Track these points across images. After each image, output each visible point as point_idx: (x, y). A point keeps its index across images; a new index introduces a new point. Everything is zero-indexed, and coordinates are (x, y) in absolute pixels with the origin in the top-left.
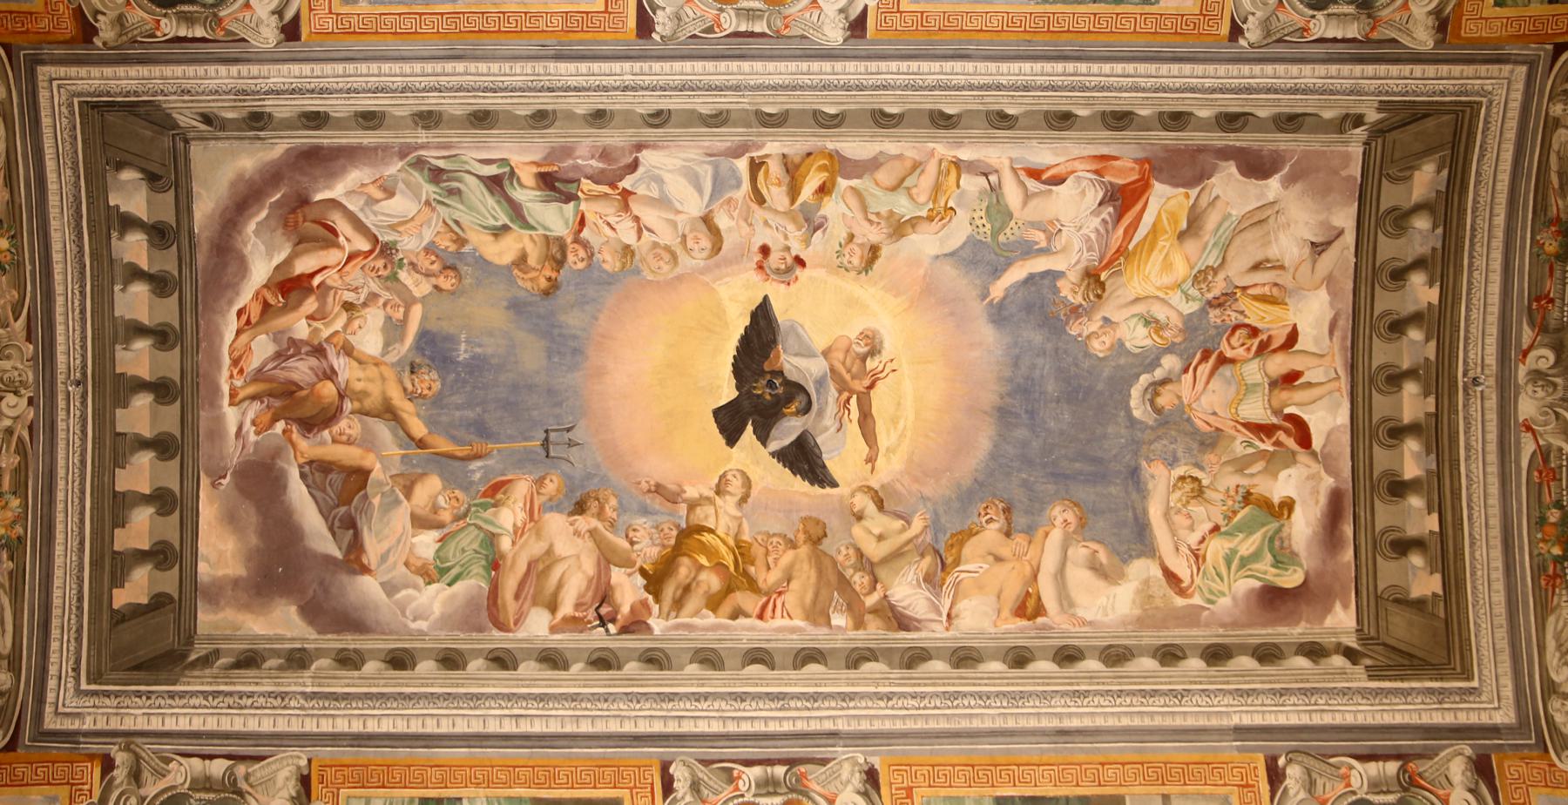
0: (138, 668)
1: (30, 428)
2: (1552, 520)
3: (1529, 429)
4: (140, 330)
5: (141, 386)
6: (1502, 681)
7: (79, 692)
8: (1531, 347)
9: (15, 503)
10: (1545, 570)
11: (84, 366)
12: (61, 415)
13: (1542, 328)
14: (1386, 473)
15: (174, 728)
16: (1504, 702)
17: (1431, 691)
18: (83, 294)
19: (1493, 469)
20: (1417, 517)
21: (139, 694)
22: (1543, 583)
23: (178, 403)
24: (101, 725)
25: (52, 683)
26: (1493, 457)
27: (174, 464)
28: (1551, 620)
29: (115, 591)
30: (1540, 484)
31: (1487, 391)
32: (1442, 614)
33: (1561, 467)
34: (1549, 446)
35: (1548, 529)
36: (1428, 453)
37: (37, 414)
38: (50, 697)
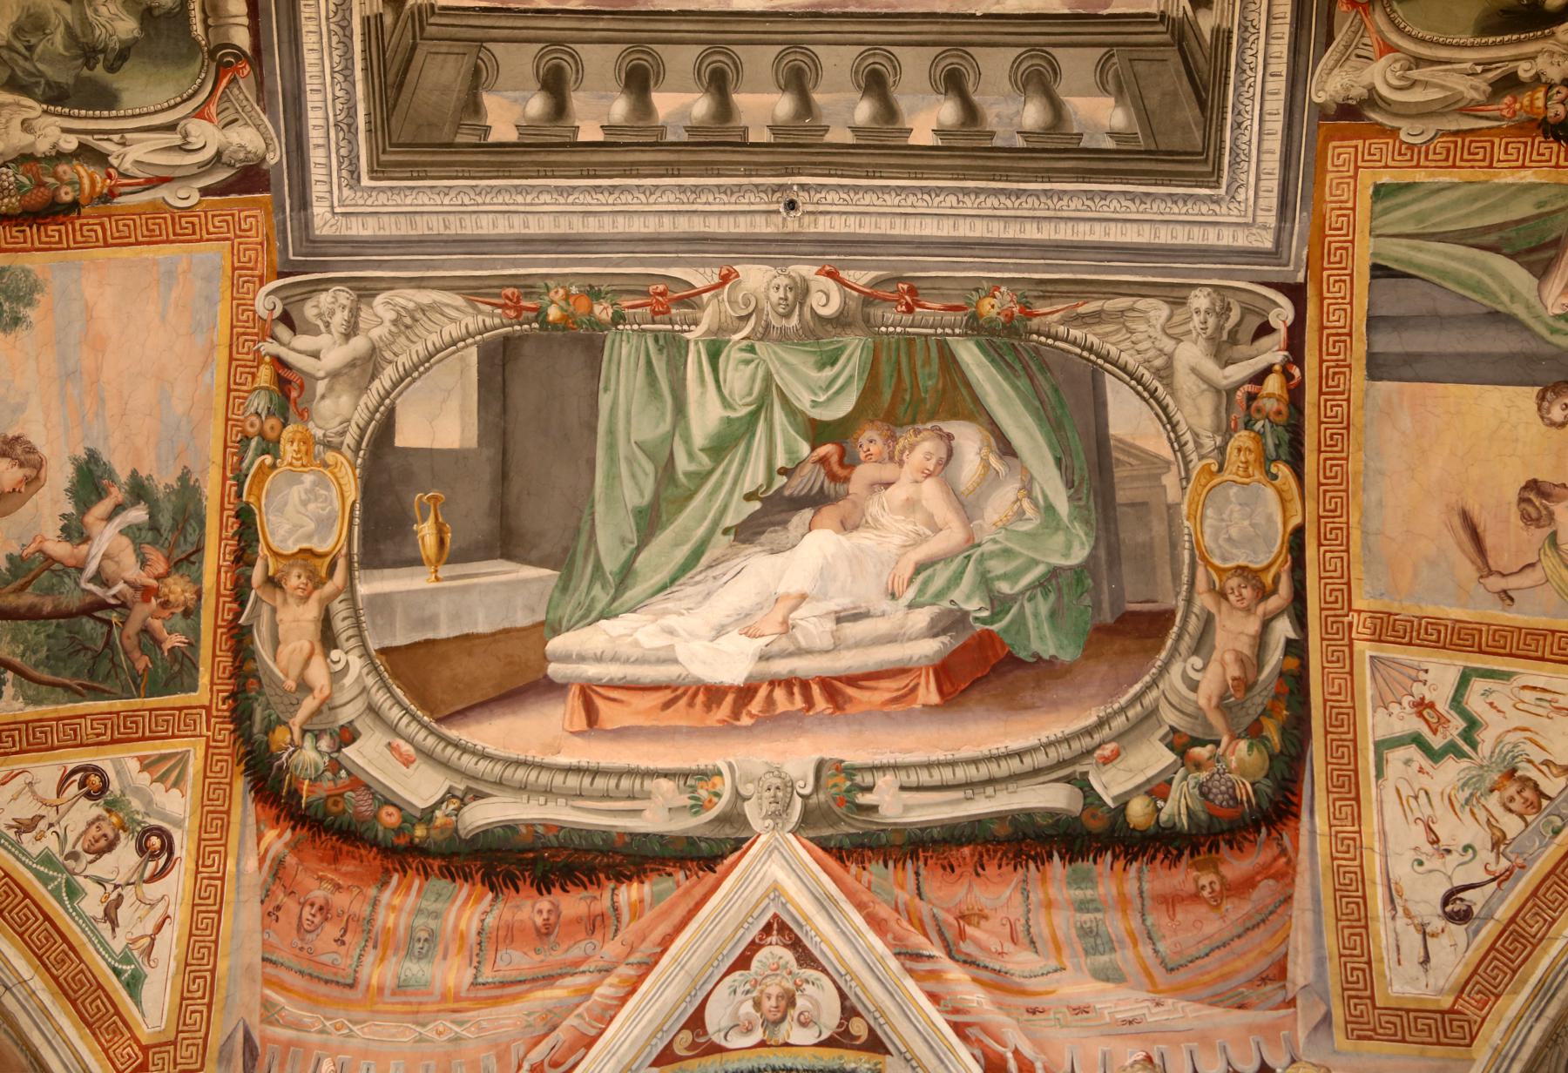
2: (597, 309)
3: (725, 279)
6: (371, 222)
8: (842, 283)
10: (528, 295)
13: (868, 299)
14: (660, 63)
16: (343, 220)
17: (351, 112)
19: (667, 226)
20: (598, 110)
22: (509, 291)
26: (684, 225)
28: (459, 301)
30: (646, 294)
31: (778, 219)
32: (460, 139)
33: (671, 322)
34: (702, 308)
35: (584, 302)
36: (689, 129)
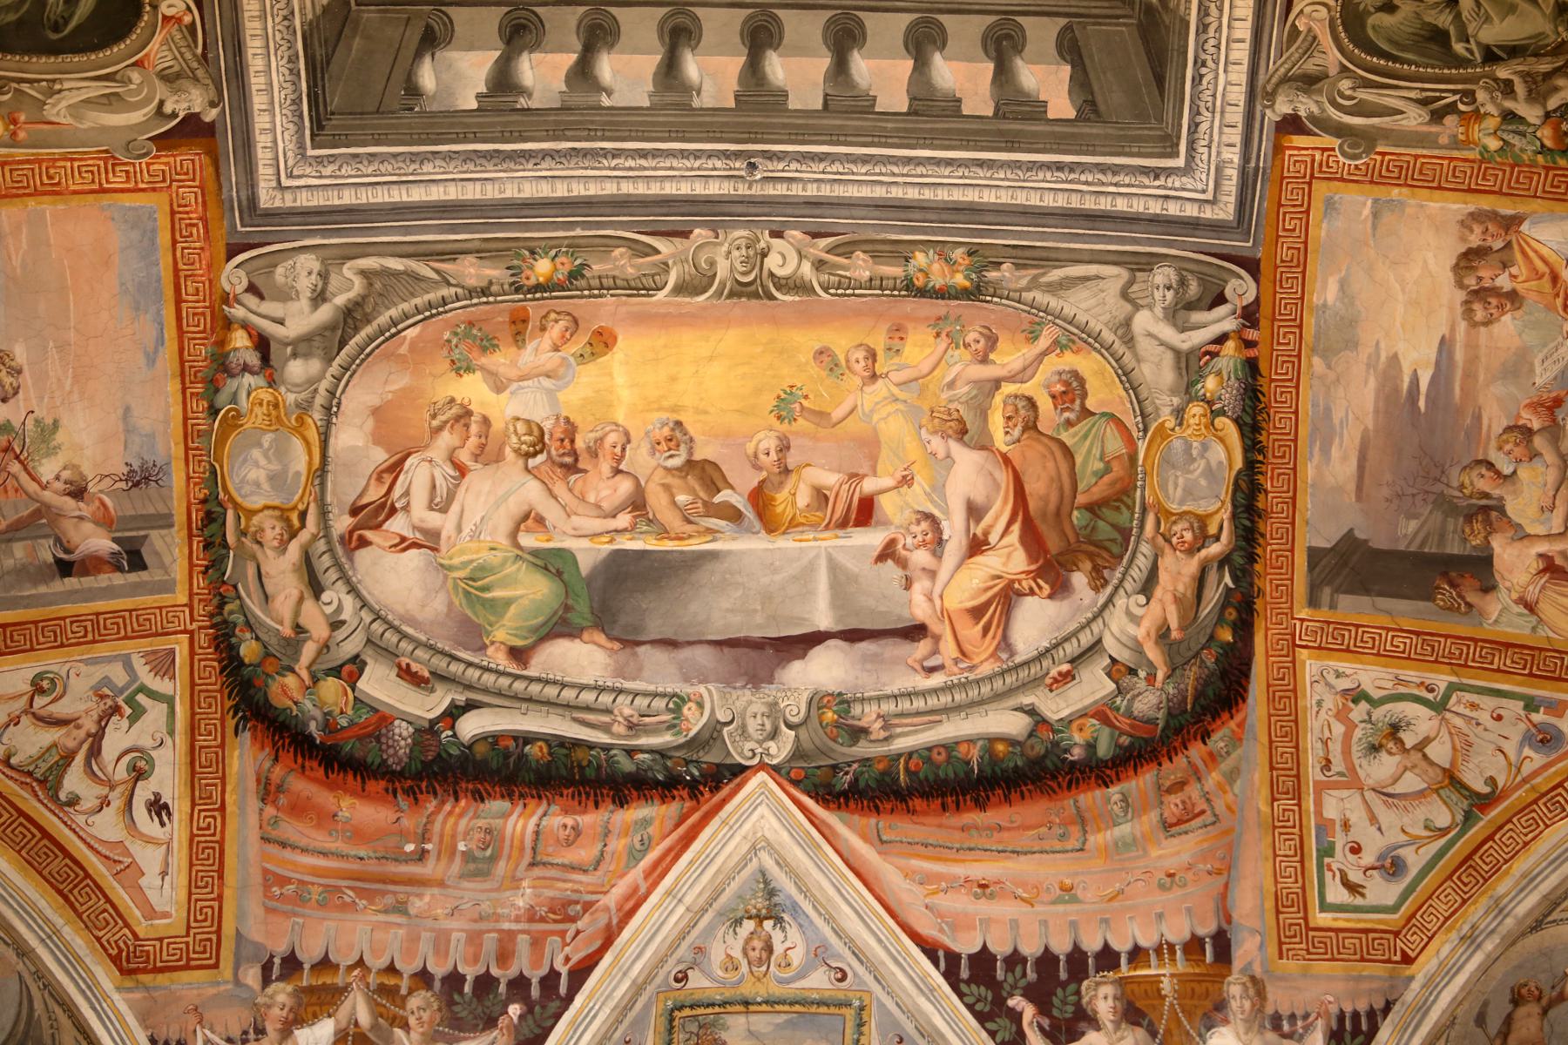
0: (1160, 80)
1: (815, 235)
4: (670, 69)
5: (754, 69)
7: (1188, 170)
9: (920, 259)
11: (726, 155)
12: (796, 190)
15: (1249, 24)
18: (616, 154)
21: (1198, 79)
23: (780, 13)
24: (1235, 136)
25: (1173, 209)
27: (870, 19)
29: (1050, 115)
37: (795, 226)
38: (1191, 211)
